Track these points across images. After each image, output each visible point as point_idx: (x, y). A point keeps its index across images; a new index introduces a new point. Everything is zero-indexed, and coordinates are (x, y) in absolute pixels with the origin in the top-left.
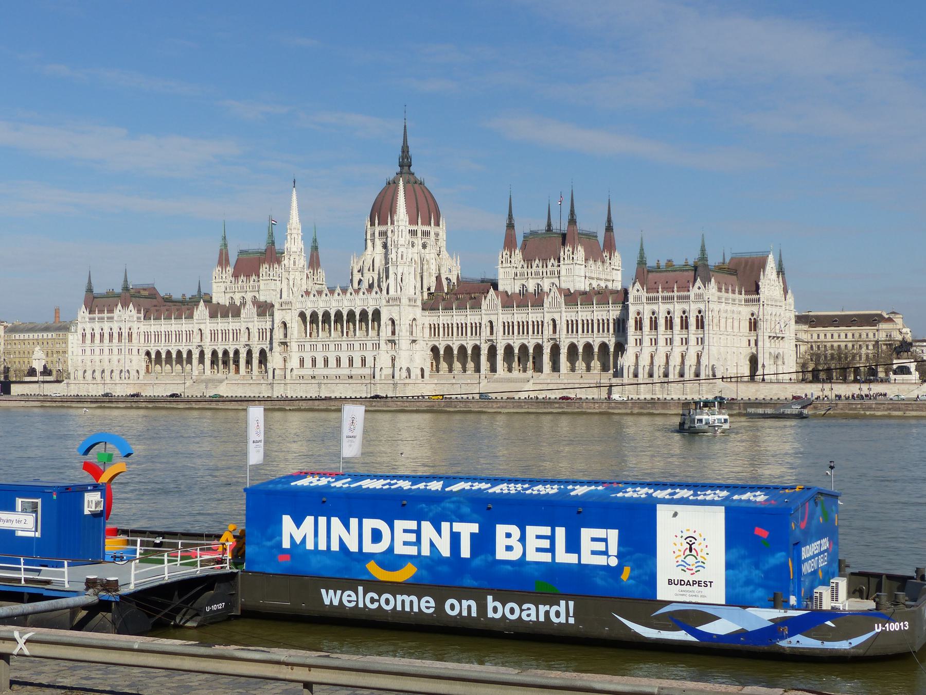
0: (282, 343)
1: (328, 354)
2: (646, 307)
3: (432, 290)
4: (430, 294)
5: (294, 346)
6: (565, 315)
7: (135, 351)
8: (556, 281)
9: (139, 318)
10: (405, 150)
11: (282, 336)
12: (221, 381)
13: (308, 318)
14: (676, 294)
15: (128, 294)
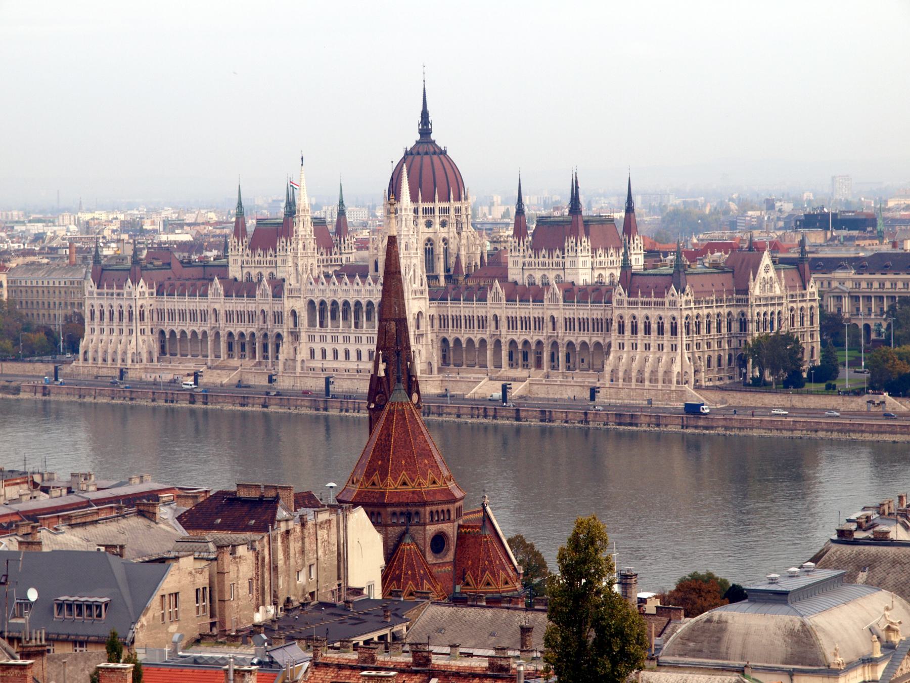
0: (292, 333)
1: (337, 347)
2: (626, 311)
3: (451, 273)
4: (446, 277)
5: (304, 336)
6: (561, 312)
7: (148, 331)
8: (561, 273)
9: (150, 294)
10: (425, 115)
11: (291, 325)
12: (236, 369)
13: (317, 308)
14: (653, 299)
15: (138, 268)
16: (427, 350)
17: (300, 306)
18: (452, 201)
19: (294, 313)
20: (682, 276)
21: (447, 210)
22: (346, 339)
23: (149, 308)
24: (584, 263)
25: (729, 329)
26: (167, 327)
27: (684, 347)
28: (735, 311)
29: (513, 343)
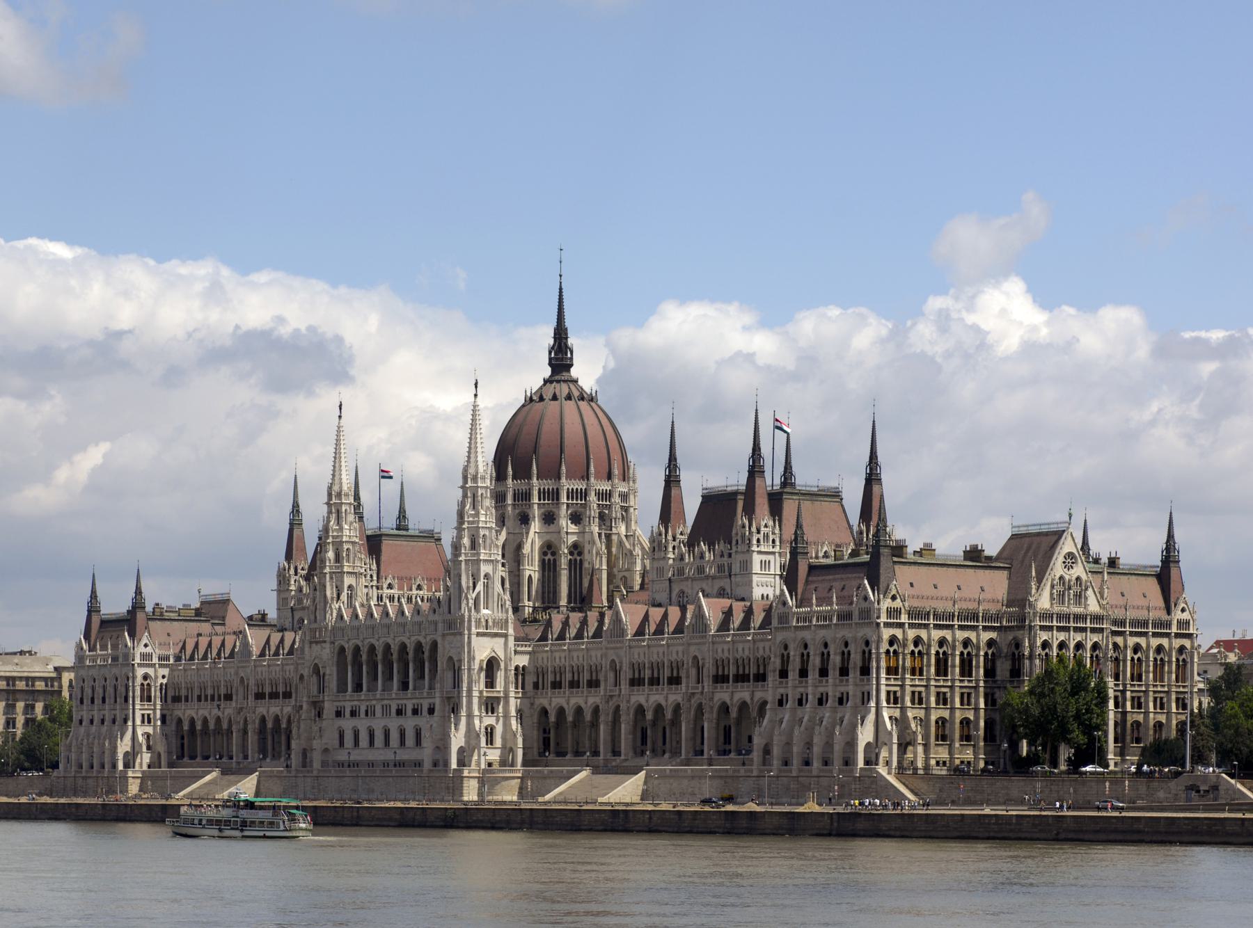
5: (329, 708)
9: (160, 659)
11: (314, 689)
16: (506, 725)
17: (325, 654)
18: (592, 479)
19: (316, 670)
20: (885, 562)
21: (584, 494)
22: (386, 710)
23: (160, 681)
24: (765, 565)
25: (990, 673)
26: (187, 712)
27: (883, 696)
28: (1005, 640)
29: (640, 710)
